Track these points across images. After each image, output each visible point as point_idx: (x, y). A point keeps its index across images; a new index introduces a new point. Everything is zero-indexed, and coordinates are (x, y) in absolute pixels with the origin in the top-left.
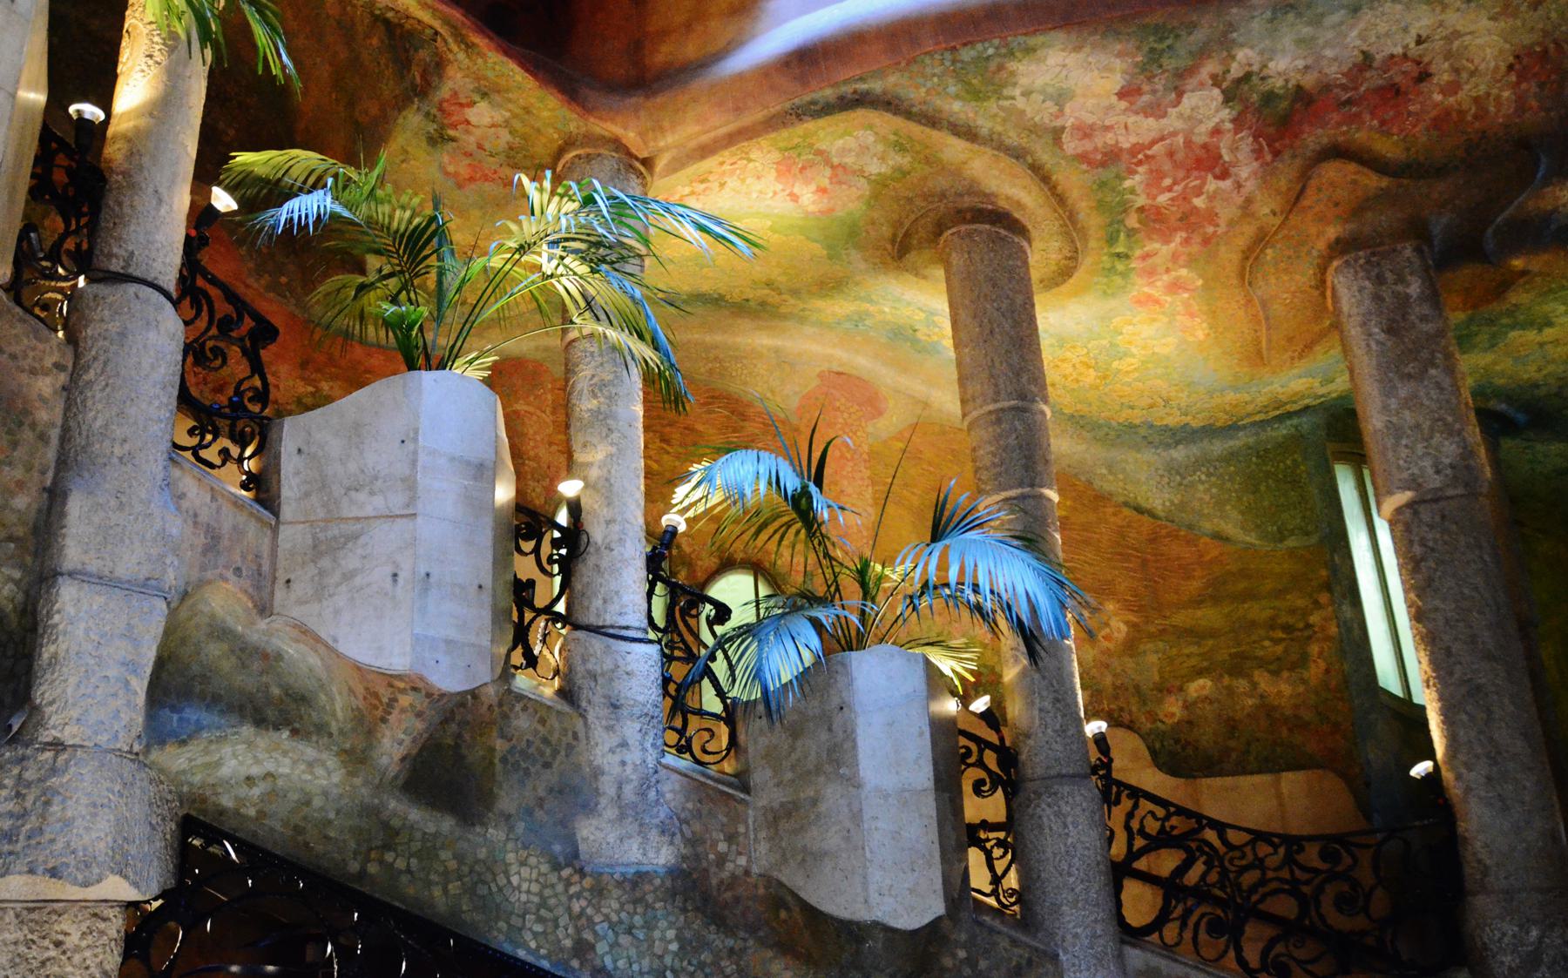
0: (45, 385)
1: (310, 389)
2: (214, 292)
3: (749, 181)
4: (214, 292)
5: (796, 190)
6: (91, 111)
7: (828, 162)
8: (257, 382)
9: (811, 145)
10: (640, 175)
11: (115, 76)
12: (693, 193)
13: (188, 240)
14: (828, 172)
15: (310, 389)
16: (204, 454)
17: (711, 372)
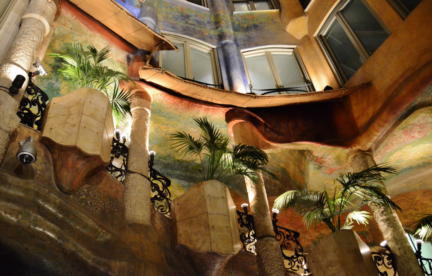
0: (256, 267)
1: (319, 234)
2: (283, 231)
3: (398, 140)
4: (283, 231)
5: (412, 135)
6: (246, 205)
7: (416, 125)
8: (299, 247)
9: (409, 124)
10: (368, 154)
11: (247, 193)
12: (386, 149)
13: (273, 221)
14: (418, 127)
15: (319, 234)
16: (293, 268)
17: (420, 186)
